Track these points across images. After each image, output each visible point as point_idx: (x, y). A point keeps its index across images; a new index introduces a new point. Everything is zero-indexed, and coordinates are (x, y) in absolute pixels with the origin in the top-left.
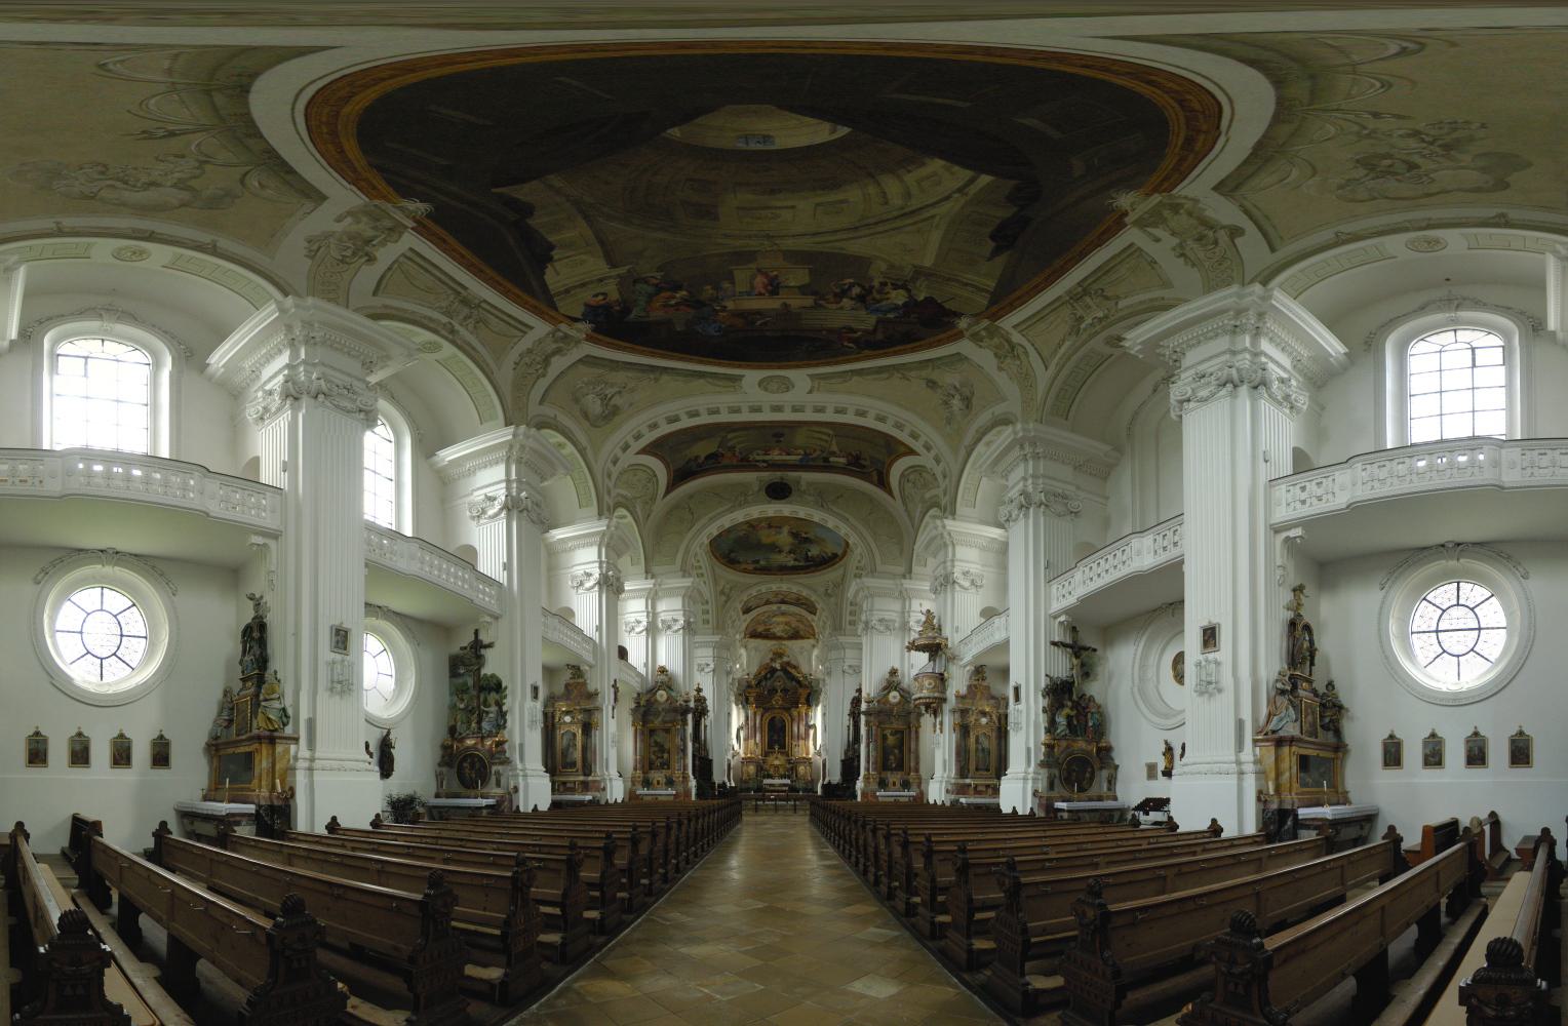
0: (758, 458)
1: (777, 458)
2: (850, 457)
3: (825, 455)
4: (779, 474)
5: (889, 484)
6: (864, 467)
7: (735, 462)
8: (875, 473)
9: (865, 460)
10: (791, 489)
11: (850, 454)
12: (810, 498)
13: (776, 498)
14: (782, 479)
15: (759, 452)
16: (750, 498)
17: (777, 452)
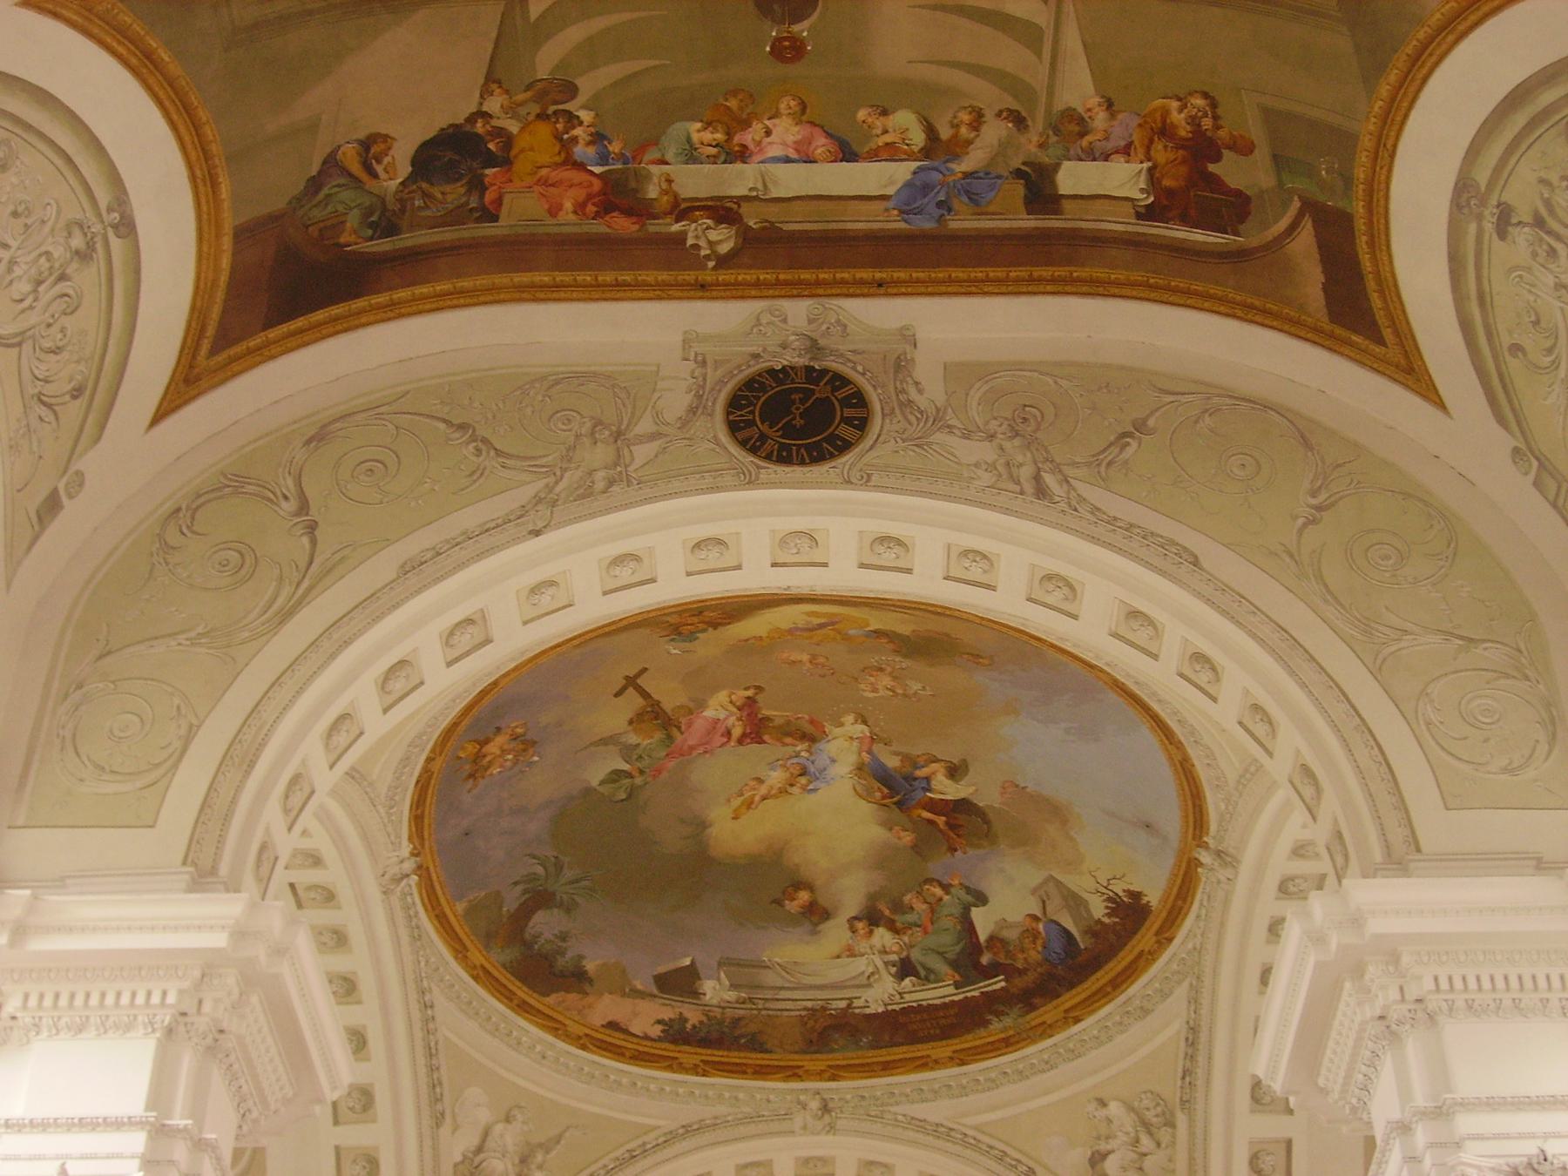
0: (695, 181)
1: (792, 180)
2: (1161, 153)
3: (1029, 146)
4: (798, 311)
5: (1389, 288)
6: (1231, 209)
7: (568, 220)
8: (1305, 243)
9: (1244, 148)
11: (1165, 131)
13: (784, 457)
14: (814, 347)
16: (642, 452)
17: (785, 132)
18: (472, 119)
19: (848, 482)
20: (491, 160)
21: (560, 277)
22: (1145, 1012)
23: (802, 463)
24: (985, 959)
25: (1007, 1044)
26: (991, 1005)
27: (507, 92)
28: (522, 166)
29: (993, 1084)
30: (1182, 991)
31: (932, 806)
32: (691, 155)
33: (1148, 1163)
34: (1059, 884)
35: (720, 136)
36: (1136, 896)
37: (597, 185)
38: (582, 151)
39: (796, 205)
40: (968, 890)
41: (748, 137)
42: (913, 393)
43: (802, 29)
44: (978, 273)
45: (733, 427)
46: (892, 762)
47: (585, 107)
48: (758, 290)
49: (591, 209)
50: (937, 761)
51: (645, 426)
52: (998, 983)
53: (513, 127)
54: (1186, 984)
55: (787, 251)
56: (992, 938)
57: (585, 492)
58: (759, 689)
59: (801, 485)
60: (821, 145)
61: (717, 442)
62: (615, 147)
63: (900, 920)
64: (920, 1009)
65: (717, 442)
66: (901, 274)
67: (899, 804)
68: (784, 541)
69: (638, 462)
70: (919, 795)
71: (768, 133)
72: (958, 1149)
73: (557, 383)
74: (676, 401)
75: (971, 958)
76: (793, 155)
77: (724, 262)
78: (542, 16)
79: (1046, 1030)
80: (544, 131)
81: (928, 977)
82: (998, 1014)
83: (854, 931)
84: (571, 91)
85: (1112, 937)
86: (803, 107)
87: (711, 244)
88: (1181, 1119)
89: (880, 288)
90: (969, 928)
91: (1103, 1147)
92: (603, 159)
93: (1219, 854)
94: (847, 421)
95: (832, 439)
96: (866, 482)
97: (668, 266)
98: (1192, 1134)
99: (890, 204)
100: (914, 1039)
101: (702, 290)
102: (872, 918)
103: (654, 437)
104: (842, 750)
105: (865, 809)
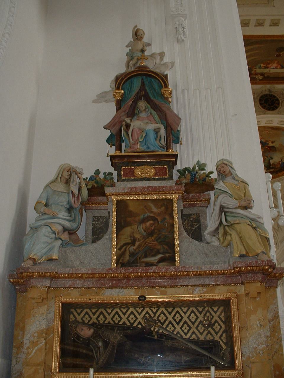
1: (273, 71)
4: (268, 86)
13: (269, 109)
14: (270, 91)
15: (262, 65)
19: (278, 113)
23: (271, 110)
24: (271, 167)
31: (268, 147)
32: (260, 68)
35: (265, 66)
40: (270, 157)
43: (281, 53)
45: (261, 104)
48: (263, 83)
50: (270, 141)
52: (273, 170)
56: (273, 164)
59: (273, 114)
60: (279, 66)
68: (268, 121)
71: (272, 65)
76: (275, 68)
77: (260, 80)
79: (279, 176)
86: (278, 62)
87: (259, 78)
90: (270, 162)
95: (275, 106)
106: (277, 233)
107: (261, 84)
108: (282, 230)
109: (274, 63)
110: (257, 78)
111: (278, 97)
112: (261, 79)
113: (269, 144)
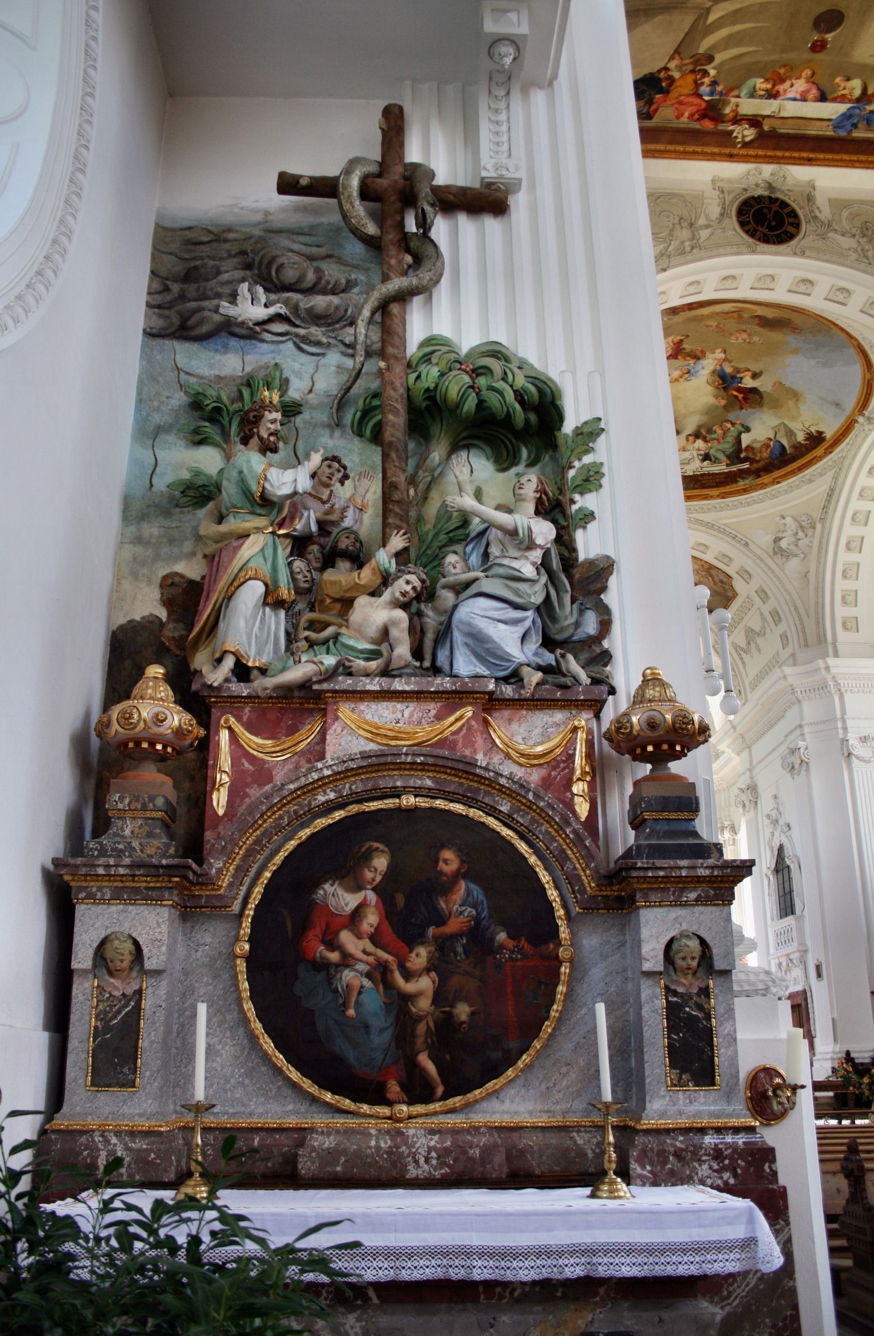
0: (748, 106)
1: (792, 109)
4: (767, 170)
7: (684, 121)
10: (794, 214)
12: (848, 243)
13: (766, 240)
14: (770, 187)
18: (660, 71)
20: (661, 91)
21: (671, 147)
22: (811, 481)
23: (774, 243)
24: (742, 455)
25: (745, 491)
26: (742, 474)
27: (681, 59)
28: (673, 95)
29: (736, 507)
30: (830, 474)
31: (740, 390)
32: (752, 95)
33: (800, 543)
34: (785, 426)
35: (769, 86)
36: (820, 433)
37: (704, 105)
38: (704, 89)
39: (789, 122)
40: (743, 426)
41: (781, 88)
42: (817, 211)
44: (855, 158)
45: (742, 224)
46: (728, 369)
47: (714, 68)
48: (756, 159)
49: (696, 116)
50: (748, 370)
51: (702, 221)
52: (746, 466)
53: (677, 75)
54: (833, 471)
55: (780, 142)
56: (748, 447)
57: (683, 253)
58: (687, 336)
61: (735, 229)
62: (719, 88)
63: (709, 437)
64: (709, 474)
65: (735, 229)
66: (821, 156)
67: (725, 389)
69: (703, 239)
70: (735, 385)
71: (792, 86)
72: (715, 533)
73: (659, 197)
74: (715, 211)
75: (736, 454)
76: (798, 97)
77: (745, 145)
78: (713, 23)
79: (763, 486)
80: (690, 78)
81: (716, 461)
82: (743, 478)
83: (687, 440)
84: (710, 59)
85: (803, 449)
86: (813, 74)
87: (743, 136)
88: (819, 526)
89: (810, 162)
90: (739, 441)
91: (781, 535)
92: (712, 93)
93: (869, 419)
94: (791, 224)
95: (786, 232)
96: (803, 254)
97: (719, 146)
98: (822, 532)
99: (831, 123)
100: (704, 487)
101: (731, 157)
102: (697, 435)
103: (707, 227)
104: (708, 365)
105: (710, 389)
106: (741, 659)
107: (745, 159)
108: (759, 650)
109: (799, 78)
110: (736, 137)
111: (793, 205)
112: (752, 142)
113: (744, 381)
